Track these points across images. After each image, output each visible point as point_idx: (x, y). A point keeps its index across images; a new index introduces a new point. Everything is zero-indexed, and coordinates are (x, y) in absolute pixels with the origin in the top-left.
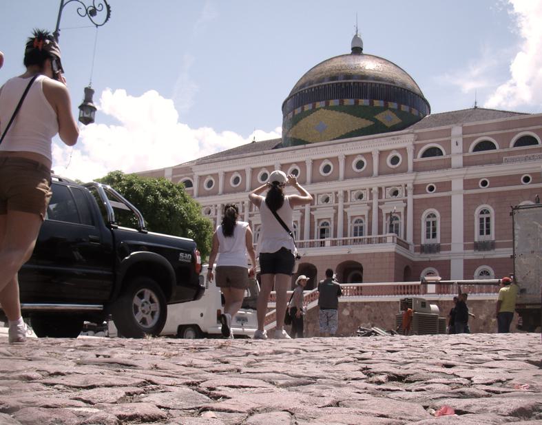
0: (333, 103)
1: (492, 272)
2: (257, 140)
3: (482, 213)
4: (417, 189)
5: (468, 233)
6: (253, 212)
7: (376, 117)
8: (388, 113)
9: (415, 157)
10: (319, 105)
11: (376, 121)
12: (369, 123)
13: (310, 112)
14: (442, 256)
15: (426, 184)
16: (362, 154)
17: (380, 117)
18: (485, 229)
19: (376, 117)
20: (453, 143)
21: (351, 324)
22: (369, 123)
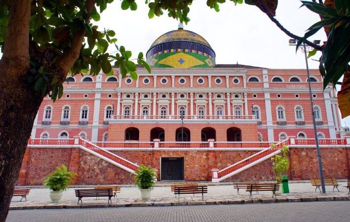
0: (186, 50)
1: (324, 136)
2: (239, 64)
3: (279, 109)
4: (249, 95)
5: (274, 118)
6: (159, 98)
7: (205, 61)
8: (209, 60)
9: (246, 81)
10: (179, 50)
11: (206, 63)
12: (202, 63)
13: (173, 53)
14: (324, 126)
15: (276, 94)
16: (202, 76)
17: (207, 61)
18: (281, 116)
19: (205, 61)
20: (264, 76)
21: (307, 159)
22: (202, 63)
